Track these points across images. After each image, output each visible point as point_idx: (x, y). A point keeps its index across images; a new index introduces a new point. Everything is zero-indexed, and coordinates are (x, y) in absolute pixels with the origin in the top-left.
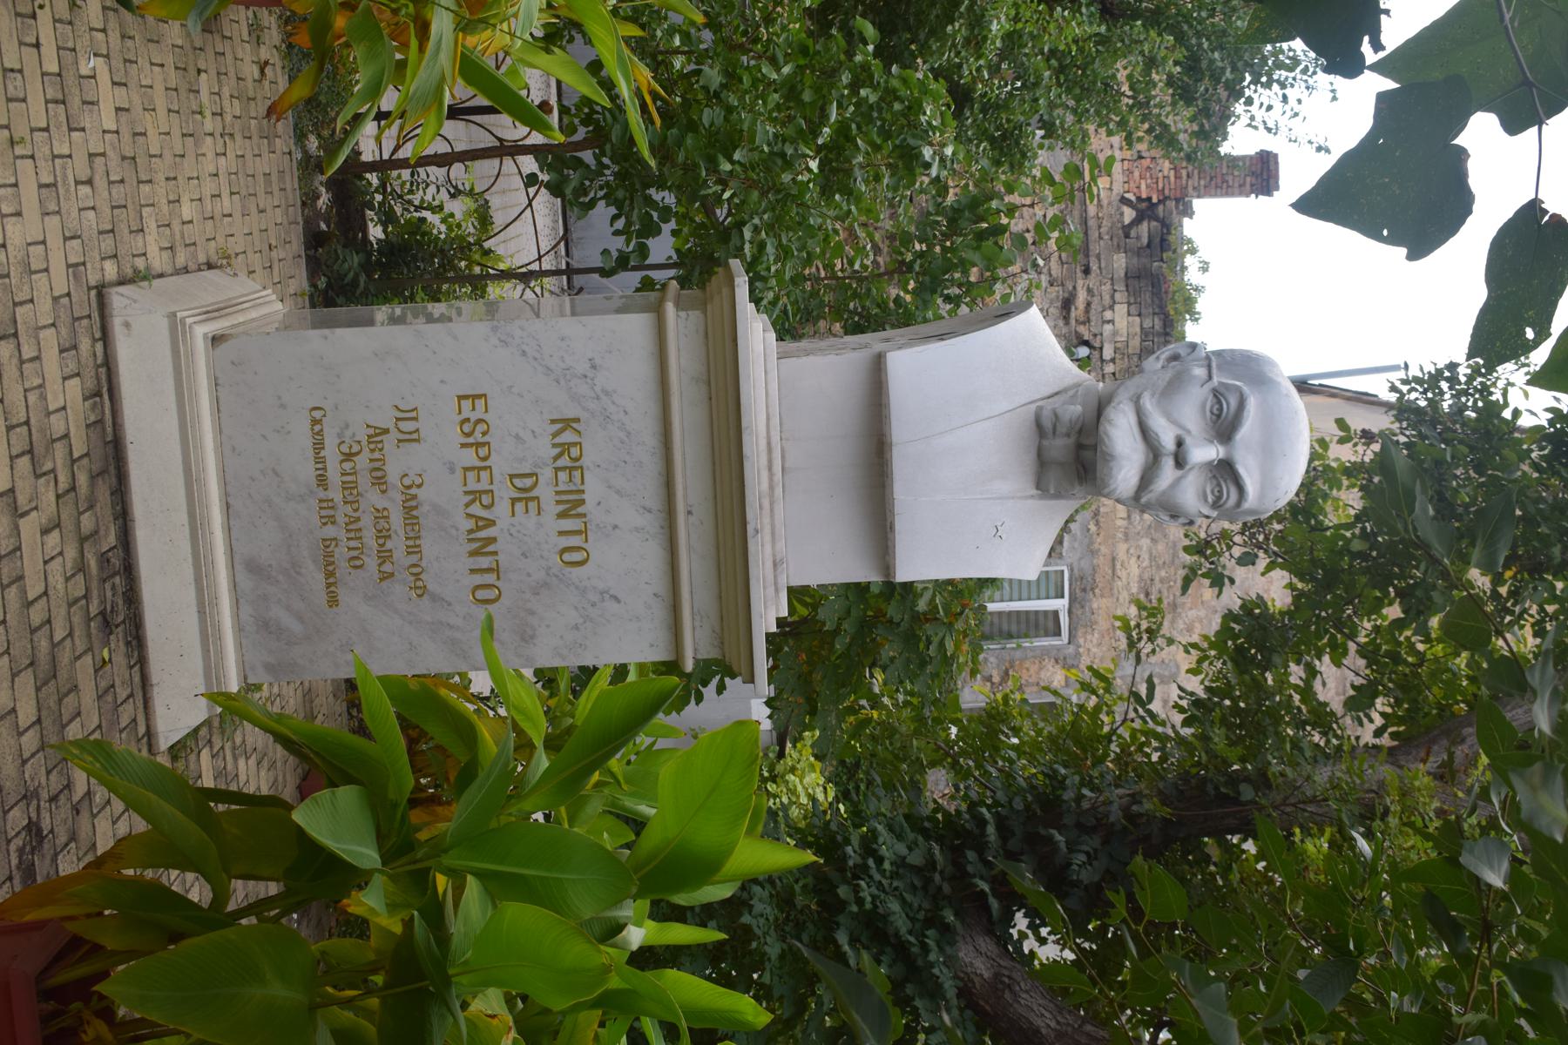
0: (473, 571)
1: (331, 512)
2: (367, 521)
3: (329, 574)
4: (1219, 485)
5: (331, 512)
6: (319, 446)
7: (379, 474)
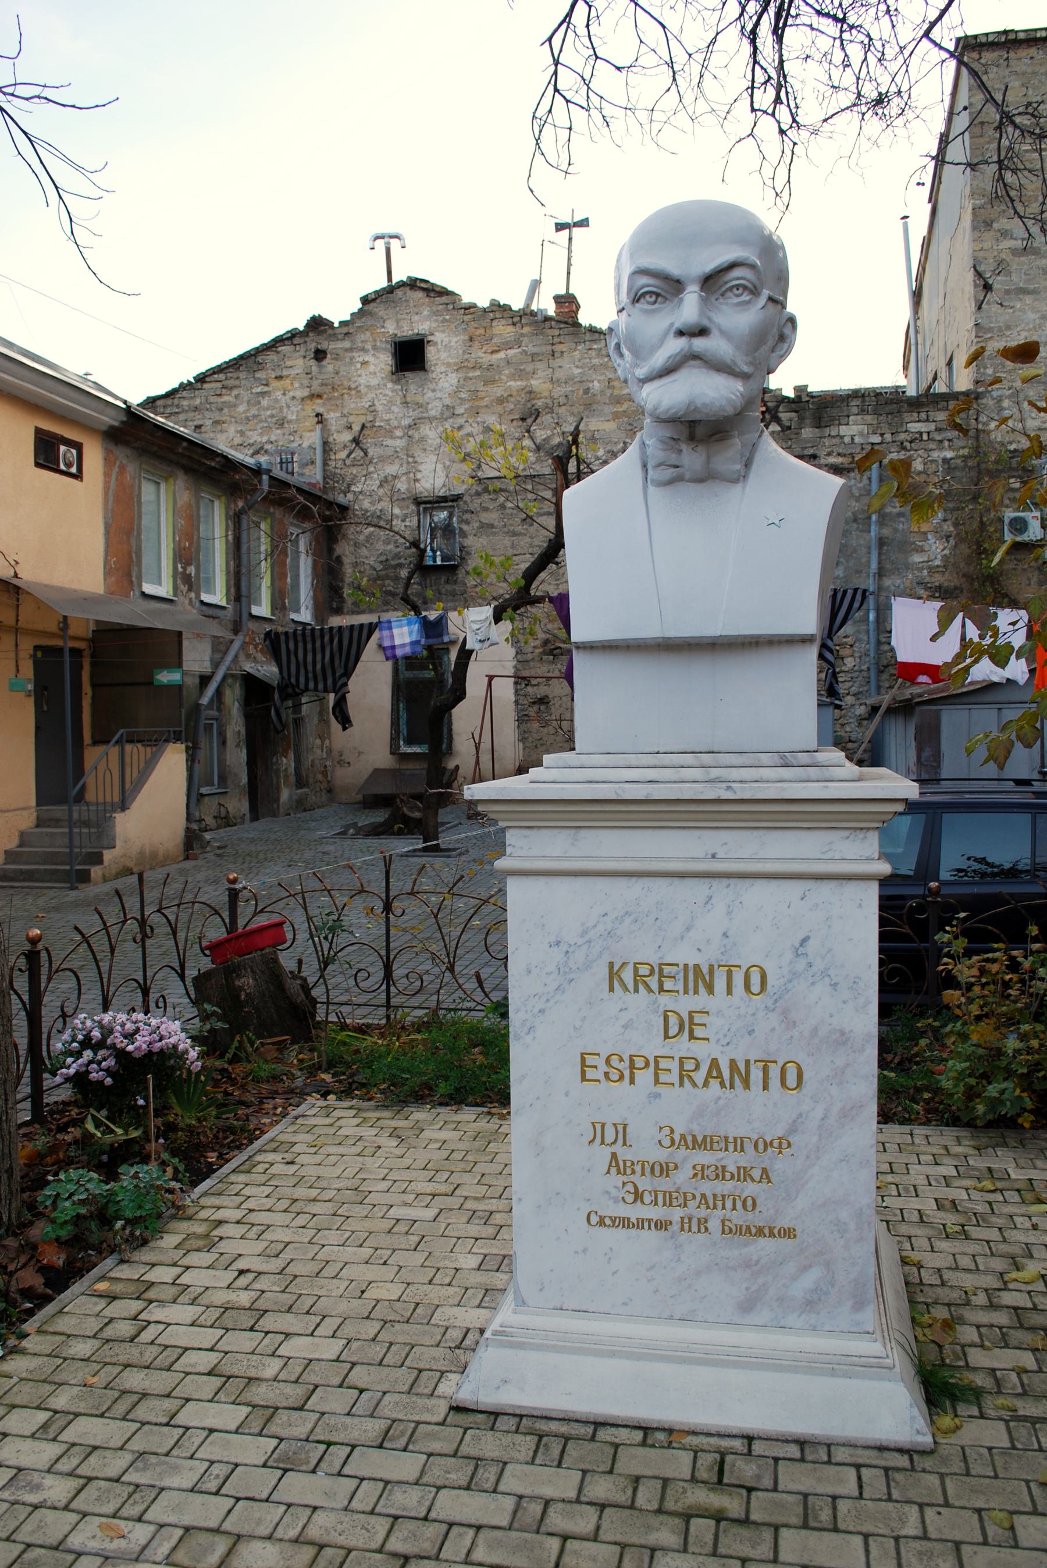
0: (765, 1087)
1: (694, 1222)
2: (707, 1187)
3: (760, 1232)
4: (731, 289)
5: (694, 1222)
6: (625, 1223)
7: (657, 1168)
